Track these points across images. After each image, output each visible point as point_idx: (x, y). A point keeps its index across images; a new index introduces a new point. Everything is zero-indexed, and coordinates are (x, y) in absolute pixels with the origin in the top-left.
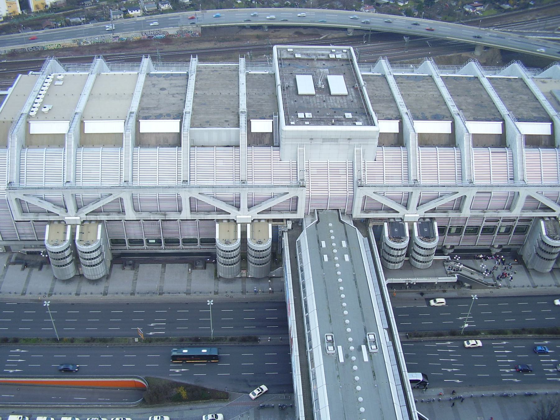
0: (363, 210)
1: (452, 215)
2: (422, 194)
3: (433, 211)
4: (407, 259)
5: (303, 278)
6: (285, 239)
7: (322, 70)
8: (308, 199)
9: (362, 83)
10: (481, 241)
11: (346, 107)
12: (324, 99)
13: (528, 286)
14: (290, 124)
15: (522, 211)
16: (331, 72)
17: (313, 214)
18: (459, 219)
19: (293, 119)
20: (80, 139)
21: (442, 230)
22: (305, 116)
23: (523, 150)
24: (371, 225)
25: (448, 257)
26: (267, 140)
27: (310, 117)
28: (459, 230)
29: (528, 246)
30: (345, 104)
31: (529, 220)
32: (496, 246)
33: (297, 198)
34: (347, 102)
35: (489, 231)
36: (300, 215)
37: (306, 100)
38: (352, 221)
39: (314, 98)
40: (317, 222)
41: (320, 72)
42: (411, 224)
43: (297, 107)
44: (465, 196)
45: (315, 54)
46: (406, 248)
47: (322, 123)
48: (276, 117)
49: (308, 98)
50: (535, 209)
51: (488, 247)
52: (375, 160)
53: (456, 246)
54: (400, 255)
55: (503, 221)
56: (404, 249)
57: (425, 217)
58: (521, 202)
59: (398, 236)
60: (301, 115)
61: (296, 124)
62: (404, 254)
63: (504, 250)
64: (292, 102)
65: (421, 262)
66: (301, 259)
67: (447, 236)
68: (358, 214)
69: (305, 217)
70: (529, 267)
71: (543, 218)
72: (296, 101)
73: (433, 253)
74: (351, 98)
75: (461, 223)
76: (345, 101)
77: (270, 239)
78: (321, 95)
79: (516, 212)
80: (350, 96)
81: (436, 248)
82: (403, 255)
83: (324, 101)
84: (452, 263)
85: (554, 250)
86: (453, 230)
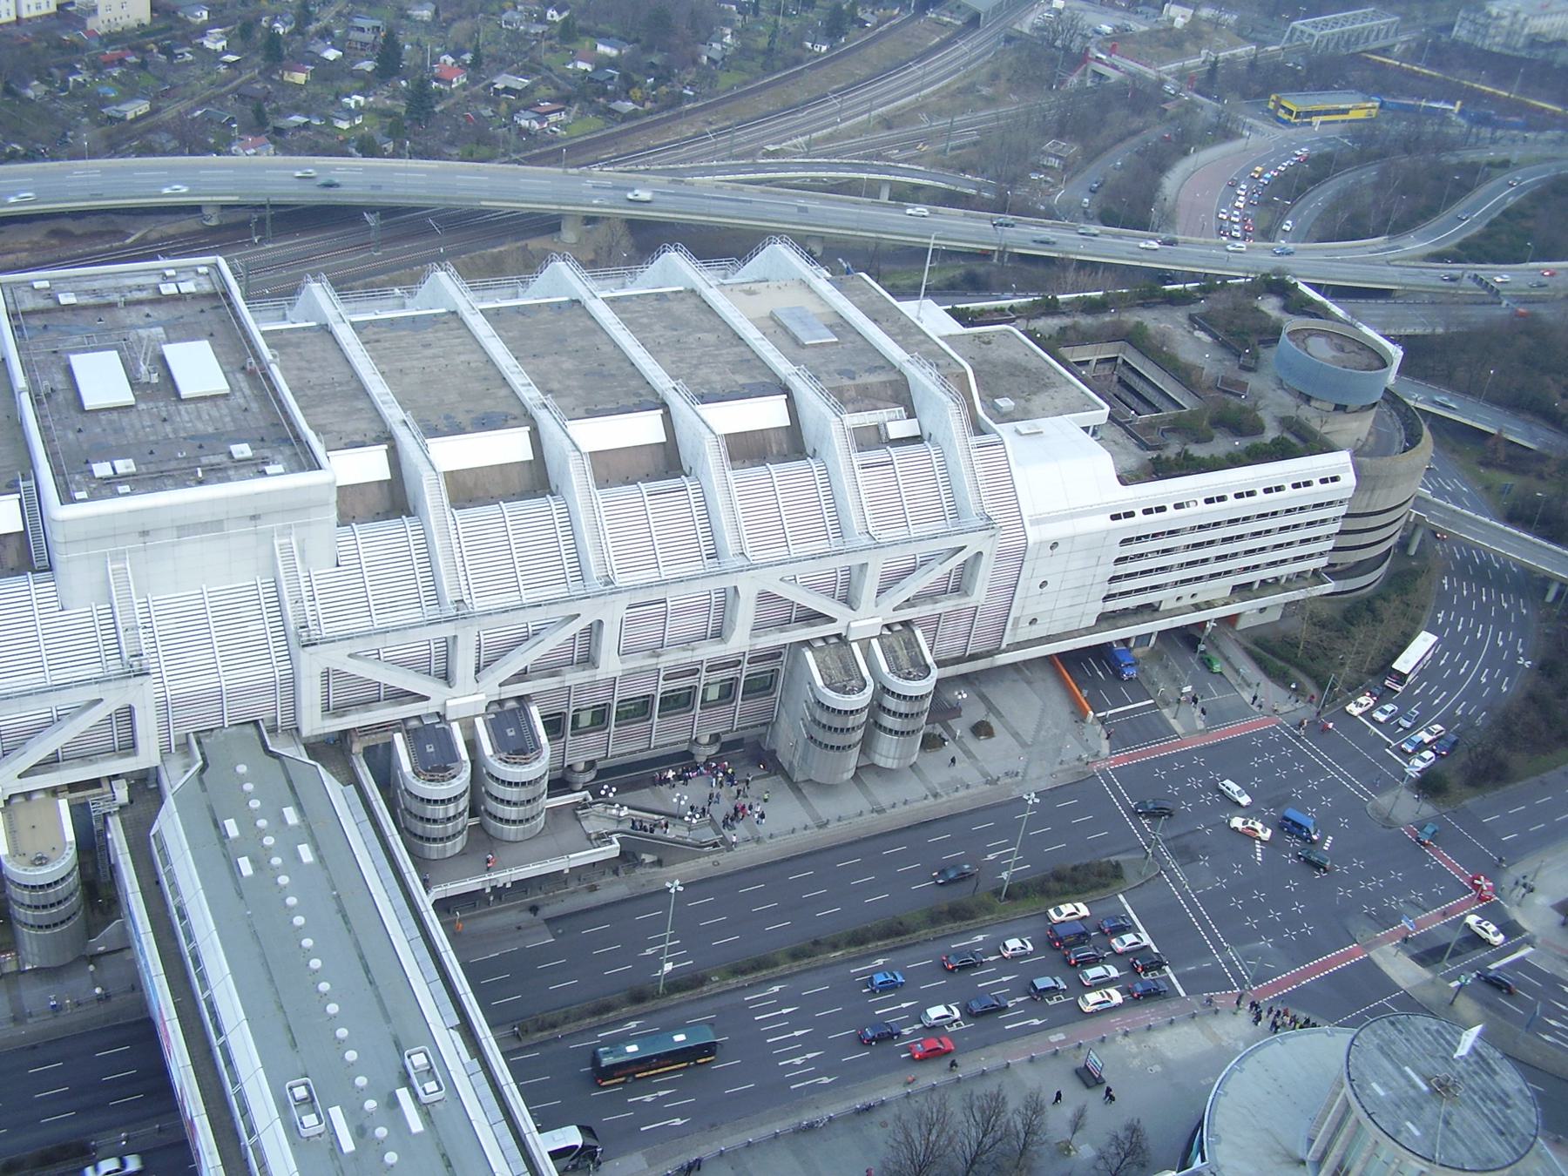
0: (329, 710)
1: (574, 677)
2: (482, 637)
3: (909, 603)
4: (474, 821)
5: (190, 937)
6: (117, 835)
7: (143, 333)
8: (164, 706)
9: (267, 354)
10: (663, 734)
11: (230, 427)
12: (164, 414)
13: (806, 828)
14: (73, 501)
15: (752, 636)
16: (172, 336)
17: (184, 747)
18: (593, 685)
19: (78, 483)
20: (666, 455)
21: (554, 725)
22: (114, 469)
23: (852, 455)
24: (357, 748)
25: (584, 793)
26: (11, 558)
27: (130, 470)
28: (600, 716)
29: (784, 724)
30: (228, 419)
31: (774, 655)
32: (706, 740)
33: (130, 710)
34: (231, 415)
35: (677, 702)
36: (147, 756)
37: (110, 422)
38: (302, 748)
39: (133, 415)
40: (203, 770)
41: (140, 339)
42: (468, 725)
43: (85, 446)
44: (981, 553)
45: (117, 290)
46: (465, 792)
47: (171, 481)
48: (27, 484)
49: (115, 416)
50: (784, 624)
51: (685, 747)
52: (338, 565)
53: (600, 760)
54: (454, 816)
55: (710, 669)
56: (462, 795)
57: (502, 697)
58: (746, 613)
59: (437, 764)
60: (102, 469)
61: (93, 497)
62: (464, 810)
63: (726, 747)
64: (71, 436)
65: (514, 822)
66: (173, 884)
67: (570, 738)
68: (315, 724)
69: (162, 761)
70: (798, 777)
71: (808, 643)
72: (80, 431)
73: (541, 791)
74: (242, 401)
75: (601, 697)
76: (225, 411)
77: (71, 843)
78: (151, 405)
79: (740, 641)
80: (238, 394)
81: (547, 777)
82: (461, 814)
83: (165, 420)
84: (599, 807)
85: (851, 721)
86: (585, 719)
